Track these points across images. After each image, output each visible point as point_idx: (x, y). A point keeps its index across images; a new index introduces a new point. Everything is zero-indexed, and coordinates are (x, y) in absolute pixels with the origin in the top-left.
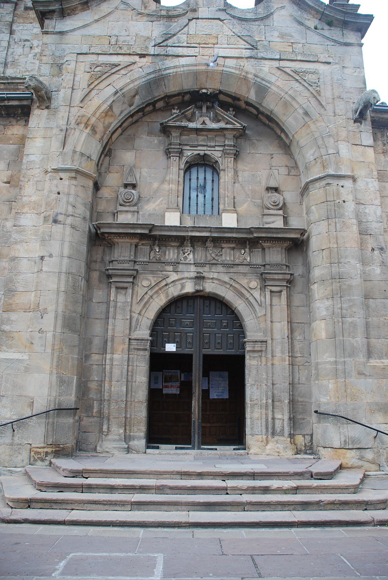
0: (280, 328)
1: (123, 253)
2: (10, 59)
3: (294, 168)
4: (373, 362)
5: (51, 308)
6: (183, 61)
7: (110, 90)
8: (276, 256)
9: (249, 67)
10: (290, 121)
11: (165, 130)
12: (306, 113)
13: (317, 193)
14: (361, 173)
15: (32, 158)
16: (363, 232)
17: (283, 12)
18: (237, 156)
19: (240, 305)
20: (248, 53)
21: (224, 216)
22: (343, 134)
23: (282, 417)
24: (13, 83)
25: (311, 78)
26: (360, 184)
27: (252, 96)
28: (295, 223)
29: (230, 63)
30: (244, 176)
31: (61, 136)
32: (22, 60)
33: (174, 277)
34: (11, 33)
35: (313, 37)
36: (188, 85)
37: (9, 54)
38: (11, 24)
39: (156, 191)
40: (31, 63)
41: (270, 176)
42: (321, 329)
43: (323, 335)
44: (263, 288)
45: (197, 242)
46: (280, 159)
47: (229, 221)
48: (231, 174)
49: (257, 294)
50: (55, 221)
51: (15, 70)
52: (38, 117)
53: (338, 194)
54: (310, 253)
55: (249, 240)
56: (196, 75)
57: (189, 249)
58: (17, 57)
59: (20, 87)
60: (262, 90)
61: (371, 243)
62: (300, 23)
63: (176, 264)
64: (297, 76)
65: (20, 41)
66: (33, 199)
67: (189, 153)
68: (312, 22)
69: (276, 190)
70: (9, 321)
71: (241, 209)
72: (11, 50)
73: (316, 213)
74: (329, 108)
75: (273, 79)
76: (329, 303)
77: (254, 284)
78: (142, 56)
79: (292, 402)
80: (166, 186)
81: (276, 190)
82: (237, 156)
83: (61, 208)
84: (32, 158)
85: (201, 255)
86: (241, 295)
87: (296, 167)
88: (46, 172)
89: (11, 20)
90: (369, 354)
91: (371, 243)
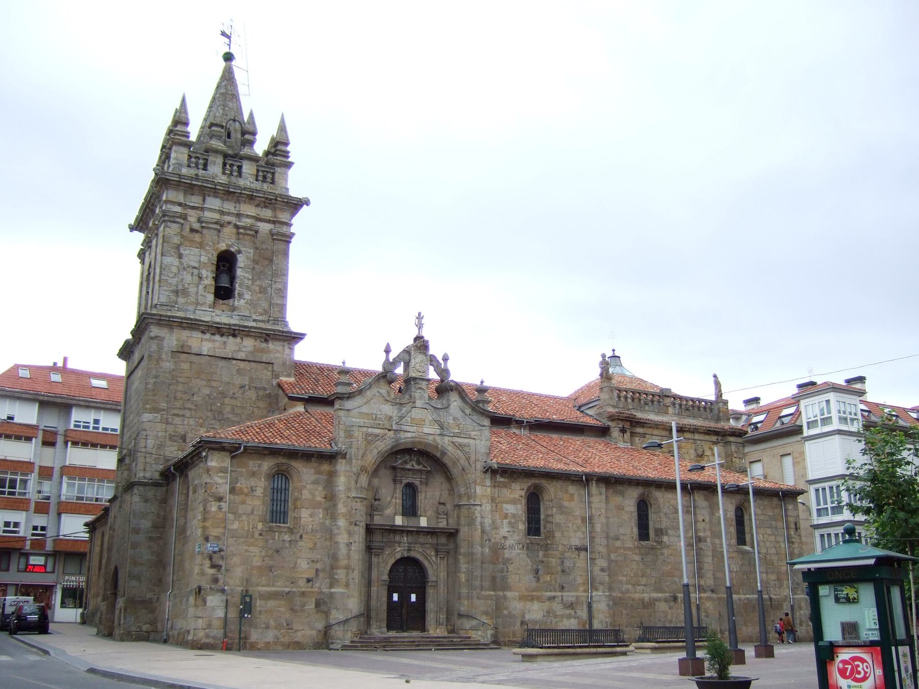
0: (443, 575)
1: (377, 537)
3: (451, 491)
4: (483, 593)
5: (357, 568)
6: (409, 435)
7: (375, 451)
8: (443, 540)
9: (438, 438)
10: (455, 471)
11: (394, 468)
12: (463, 469)
13: (464, 511)
14: (485, 501)
15: (340, 488)
16: (483, 532)
17: (455, 403)
18: (426, 484)
19: (426, 563)
20: (438, 432)
21: (421, 518)
22: (478, 481)
23: (443, 617)
25: (467, 449)
26: (483, 507)
27: (438, 455)
28: (452, 524)
29: (431, 437)
30: (429, 494)
31: (354, 478)
32: (193, 290)
33: (399, 549)
35: (469, 421)
36: (409, 446)
38: (178, 247)
39: (389, 503)
41: (441, 495)
42: (463, 577)
43: (463, 580)
44: (436, 555)
45: (408, 532)
46: (446, 486)
47: (423, 522)
48: (423, 495)
49: (434, 558)
50: (356, 525)
52: (341, 466)
53: (474, 513)
54: (458, 539)
55: (431, 532)
56: (414, 442)
57: (405, 535)
58: (186, 286)
60: (444, 453)
61: (486, 537)
62: (463, 412)
63: (399, 543)
64: (459, 447)
66: (343, 511)
67: (405, 481)
68: (468, 411)
69: (443, 504)
70: (337, 574)
71: (428, 514)
73: (463, 521)
74: (473, 465)
75: (450, 448)
76: (466, 566)
77: (433, 553)
78: (390, 430)
79: (447, 610)
80: (394, 500)
81: (443, 504)
82: (426, 484)
83: (358, 518)
84: (340, 488)
85: (411, 539)
86: (426, 558)
87: (453, 490)
88: (348, 497)
90: (482, 590)
91: (486, 537)
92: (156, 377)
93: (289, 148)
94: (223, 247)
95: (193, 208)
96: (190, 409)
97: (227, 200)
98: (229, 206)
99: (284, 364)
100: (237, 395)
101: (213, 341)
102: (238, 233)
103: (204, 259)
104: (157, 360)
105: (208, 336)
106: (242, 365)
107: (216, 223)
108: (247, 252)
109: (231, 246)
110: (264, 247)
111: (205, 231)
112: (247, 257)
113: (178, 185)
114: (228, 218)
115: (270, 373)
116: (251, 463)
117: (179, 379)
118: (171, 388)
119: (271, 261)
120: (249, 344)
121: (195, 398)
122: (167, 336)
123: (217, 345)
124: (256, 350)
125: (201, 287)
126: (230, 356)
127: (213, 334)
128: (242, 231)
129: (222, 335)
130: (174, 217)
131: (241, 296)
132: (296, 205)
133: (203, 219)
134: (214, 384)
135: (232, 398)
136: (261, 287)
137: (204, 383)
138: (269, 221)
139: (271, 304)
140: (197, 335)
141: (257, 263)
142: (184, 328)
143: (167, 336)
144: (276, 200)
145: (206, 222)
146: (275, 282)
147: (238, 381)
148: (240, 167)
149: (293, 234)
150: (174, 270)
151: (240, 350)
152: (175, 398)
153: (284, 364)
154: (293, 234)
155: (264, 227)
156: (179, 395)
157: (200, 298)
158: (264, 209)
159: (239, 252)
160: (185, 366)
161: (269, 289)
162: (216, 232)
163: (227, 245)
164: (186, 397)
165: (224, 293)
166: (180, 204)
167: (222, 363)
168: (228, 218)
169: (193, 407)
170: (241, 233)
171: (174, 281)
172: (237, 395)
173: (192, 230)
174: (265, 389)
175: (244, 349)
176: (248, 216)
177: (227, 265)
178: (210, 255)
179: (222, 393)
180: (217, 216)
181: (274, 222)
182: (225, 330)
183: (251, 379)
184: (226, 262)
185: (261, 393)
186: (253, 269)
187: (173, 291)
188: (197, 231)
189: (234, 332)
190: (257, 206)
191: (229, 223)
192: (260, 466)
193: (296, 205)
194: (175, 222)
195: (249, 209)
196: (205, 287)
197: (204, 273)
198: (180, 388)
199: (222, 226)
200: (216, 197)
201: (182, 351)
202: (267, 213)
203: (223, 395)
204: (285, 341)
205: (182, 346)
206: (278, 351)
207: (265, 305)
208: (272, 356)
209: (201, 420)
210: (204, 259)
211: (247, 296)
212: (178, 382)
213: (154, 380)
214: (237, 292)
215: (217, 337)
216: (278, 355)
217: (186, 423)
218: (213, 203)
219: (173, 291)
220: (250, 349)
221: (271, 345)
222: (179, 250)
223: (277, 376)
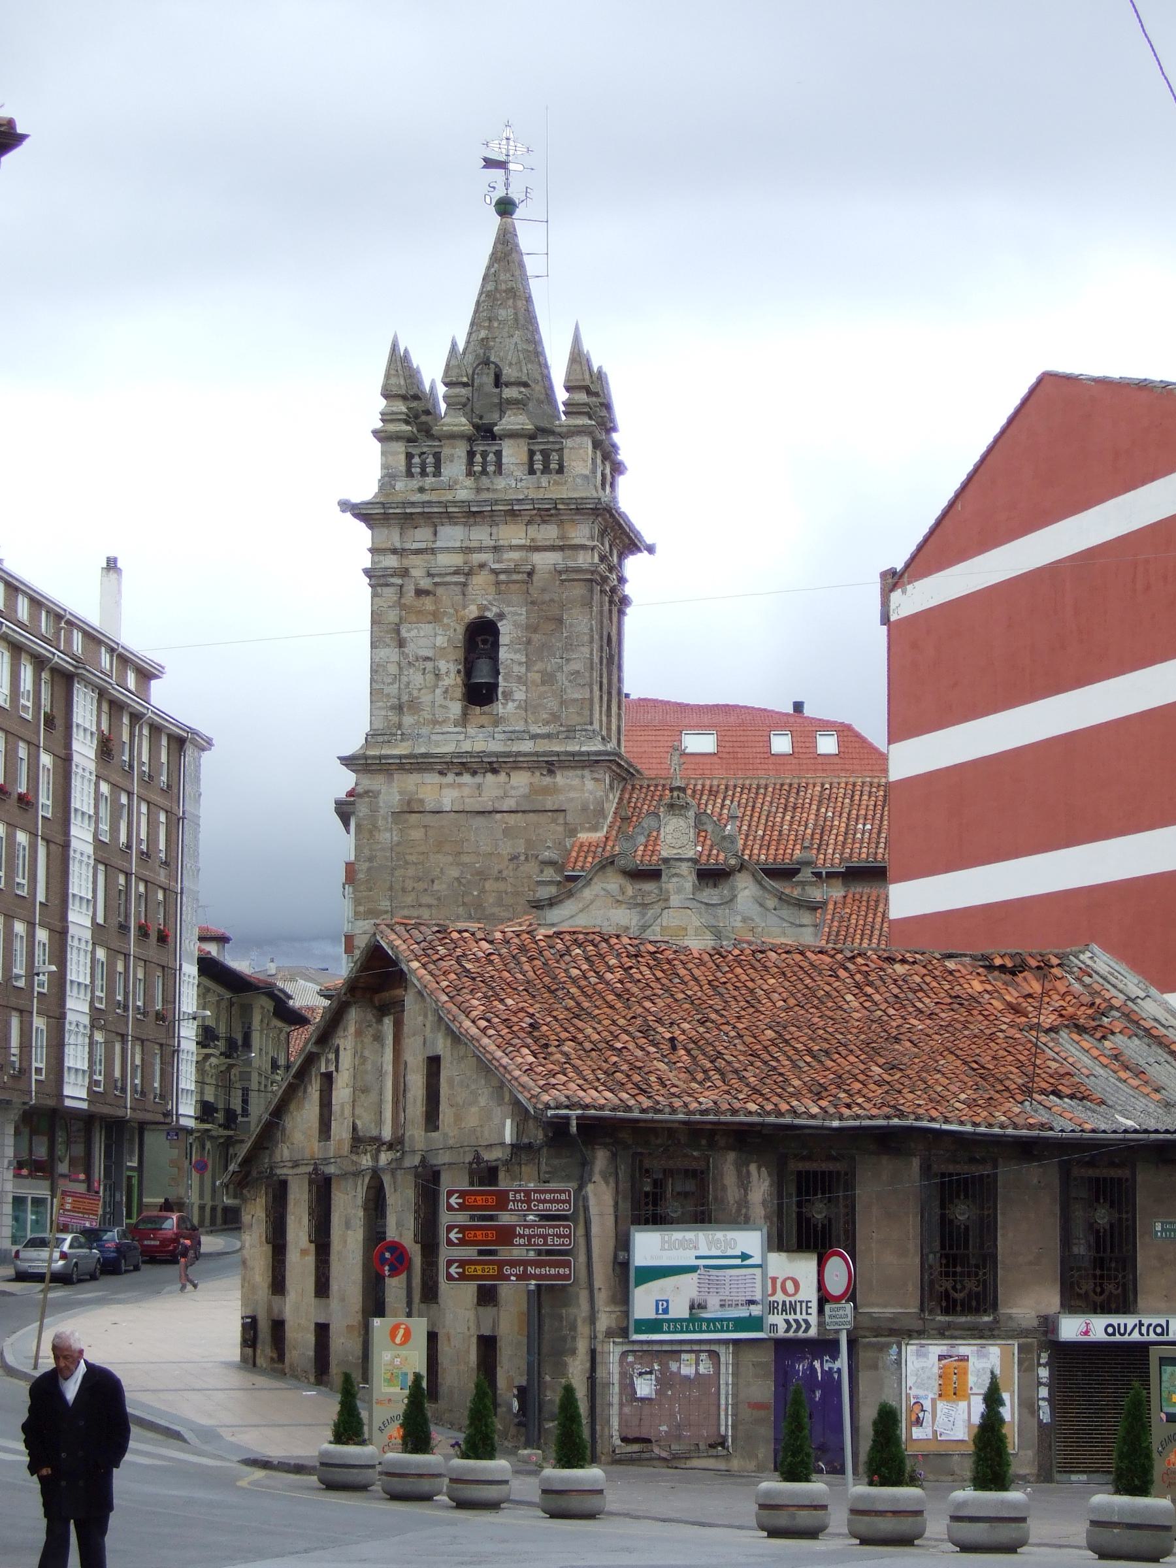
2: (405, 698)
32: (426, 698)
34: (401, 643)
37: (402, 686)
40: (441, 706)
58: (415, 693)
65: (417, 660)
72: (404, 679)
89: (397, 620)
92: (371, 859)
94: (472, 612)
95: (418, 552)
96: (429, 906)
97: (475, 524)
98: (480, 535)
99: (585, 809)
100: (505, 873)
101: (460, 785)
102: (498, 583)
103: (441, 641)
104: (371, 832)
105: (450, 778)
106: (512, 819)
107: (456, 573)
108: (516, 614)
110: (547, 597)
111: (440, 591)
112: (516, 625)
113: (388, 519)
114: (477, 558)
115: (560, 829)
117: (408, 857)
118: (397, 873)
119: (560, 621)
120: (521, 781)
121: (436, 887)
122: (384, 789)
123: (466, 791)
124: (535, 790)
125: (438, 691)
127: (457, 774)
128: (502, 577)
129: (474, 773)
131: (508, 695)
133: (433, 571)
134: (466, 859)
135: (497, 879)
136: (543, 672)
137: (450, 859)
138: (553, 548)
139: (562, 703)
140: (432, 778)
141: (535, 631)
142: (410, 771)
143: (384, 789)
144: (556, 508)
146: (568, 660)
147: (506, 848)
148: (499, 454)
150: (393, 669)
151: (506, 796)
152: (404, 890)
153: (585, 809)
155: (544, 561)
156: (409, 884)
157: (438, 711)
158: (543, 527)
159: (501, 616)
160: (416, 834)
162: (458, 589)
164: (421, 886)
165: (479, 694)
166: (394, 551)
167: (479, 821)
168: (477, 558)
169: (435, 902)
170: (503, 582)
171: (393, 690)
172: (505, 873)
173: (420, 593)
175: (513, 793)
176: (512, 548)
178: (451, 633)
179: (480, 873)
180: (457, 560)
181: (561, 548)
183: (529, 842)
184: (481, 637)
186: (529, 642)
187: (392, 708)
188: (427, 593)
189: (492, 765)
191: (482, 566)
194: (387, 585)
195: (513, 534)
196: (446, 692)
197: (443, 665)
198: (411, 872)
199: (468, 574)
200: (456, 524)
201: (410, 809)
202: (548, 533)
203: (482, 875)
204: (583, 768)
205: (409, 802)
206: (572, 788)
207: (552, 704)
208: (562, 797)
210: (441, 641)
211: (519, 695)
212: (407, 863)
213: (367, 864)
214: (500, 690)
215: (467, 778)
216: (572, 795)
218: (452, 535)
219: (392, 708)
221: (560, 779)
222: (398, 632)
223: (572, 832)
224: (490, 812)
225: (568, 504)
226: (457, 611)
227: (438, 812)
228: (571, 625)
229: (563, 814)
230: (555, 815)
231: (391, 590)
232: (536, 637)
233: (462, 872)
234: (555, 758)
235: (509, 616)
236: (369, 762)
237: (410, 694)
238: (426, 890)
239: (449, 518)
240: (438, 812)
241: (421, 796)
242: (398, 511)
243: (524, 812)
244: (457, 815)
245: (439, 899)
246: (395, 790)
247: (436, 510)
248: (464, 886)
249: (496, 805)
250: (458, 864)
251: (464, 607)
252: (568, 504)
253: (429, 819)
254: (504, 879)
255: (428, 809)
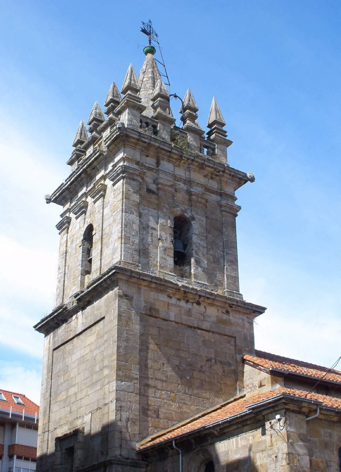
24: (164, 285)
51: (147, 260)
59: (168, 290)
92: (127, 340)
93: (224, 128)
95: (149, 169)
98: (181, 172)
102: (190, 200)
106: (207, 335)
108: (200, 220)
109: (185, 211)
113: (136, 144)
115: (232, 348)
116: (322, 431)
120: (213, 312)
124: (220, 321)
126: (196, 325)
130: (132, 174)
132: (241, 179)
133: (160, 181)
134: (183, 354)
135: (200, 371)
137: (173, 352)
140: (163, 297)
145: (162, 184)
149: (239, 208)
150: (136, 227)
154: (239, 208)
155: (214, 198)
159: (193, 219)
161: (222, 260)
163: (182, 210)
167: (189, 332)
169: (164, 379)
172: (204, 369)
173: (149, 191)
174: (230, 365)
177: (178, 232)
179: (190, 365)
181: (221, 195)
182: (191, 296)
185: (226, 368)
188: (153, 192)
190: (205, 176)
192: (330, 436)
193: (241, 179)
194: (134, 180)
195: (198, 177)
205: (151, 309)
209: (172, 395)
213: (125, 344)
215: (183, 303)
217: (158, 395)
218: (166, 165)
220: (214, 319)
224: (195, 328)
225: (230, 171)
226: (170, 207)
227: (166, 320)
228: (228, 236)
229: (233, 339)
230: (230, 339)
231: (134, 183)
232: (210, 236)
233: (180, 363)
234: (235, 303)
235: (197, 220)
236: (133, 275)
237: (144, 245)
238: (159, 370)
239: (169, 157)
240: (166, 320)
241: (157, 307)
242: (147, 141)
243: (213, 332)
244: (176, 325)
245: (167, 377)
246: (142, 299)
247: (166, 148)
248: (182, 371)
249: (200, 324)
250: (177, 356)
251: (174, 207)
252: (230, 171)
253: (160, 323)
254: (204, 372)
255: (161, 316)
